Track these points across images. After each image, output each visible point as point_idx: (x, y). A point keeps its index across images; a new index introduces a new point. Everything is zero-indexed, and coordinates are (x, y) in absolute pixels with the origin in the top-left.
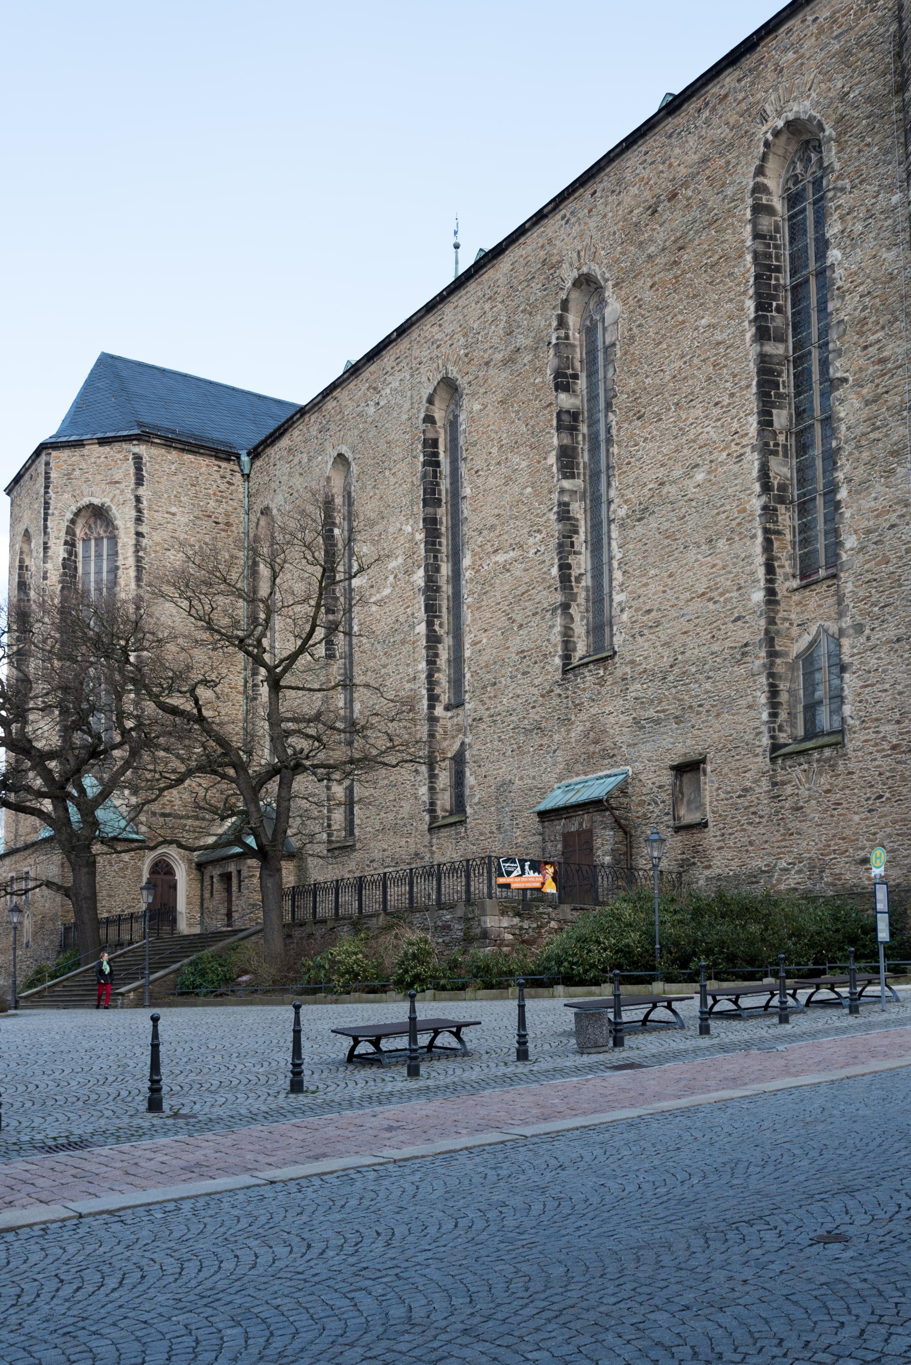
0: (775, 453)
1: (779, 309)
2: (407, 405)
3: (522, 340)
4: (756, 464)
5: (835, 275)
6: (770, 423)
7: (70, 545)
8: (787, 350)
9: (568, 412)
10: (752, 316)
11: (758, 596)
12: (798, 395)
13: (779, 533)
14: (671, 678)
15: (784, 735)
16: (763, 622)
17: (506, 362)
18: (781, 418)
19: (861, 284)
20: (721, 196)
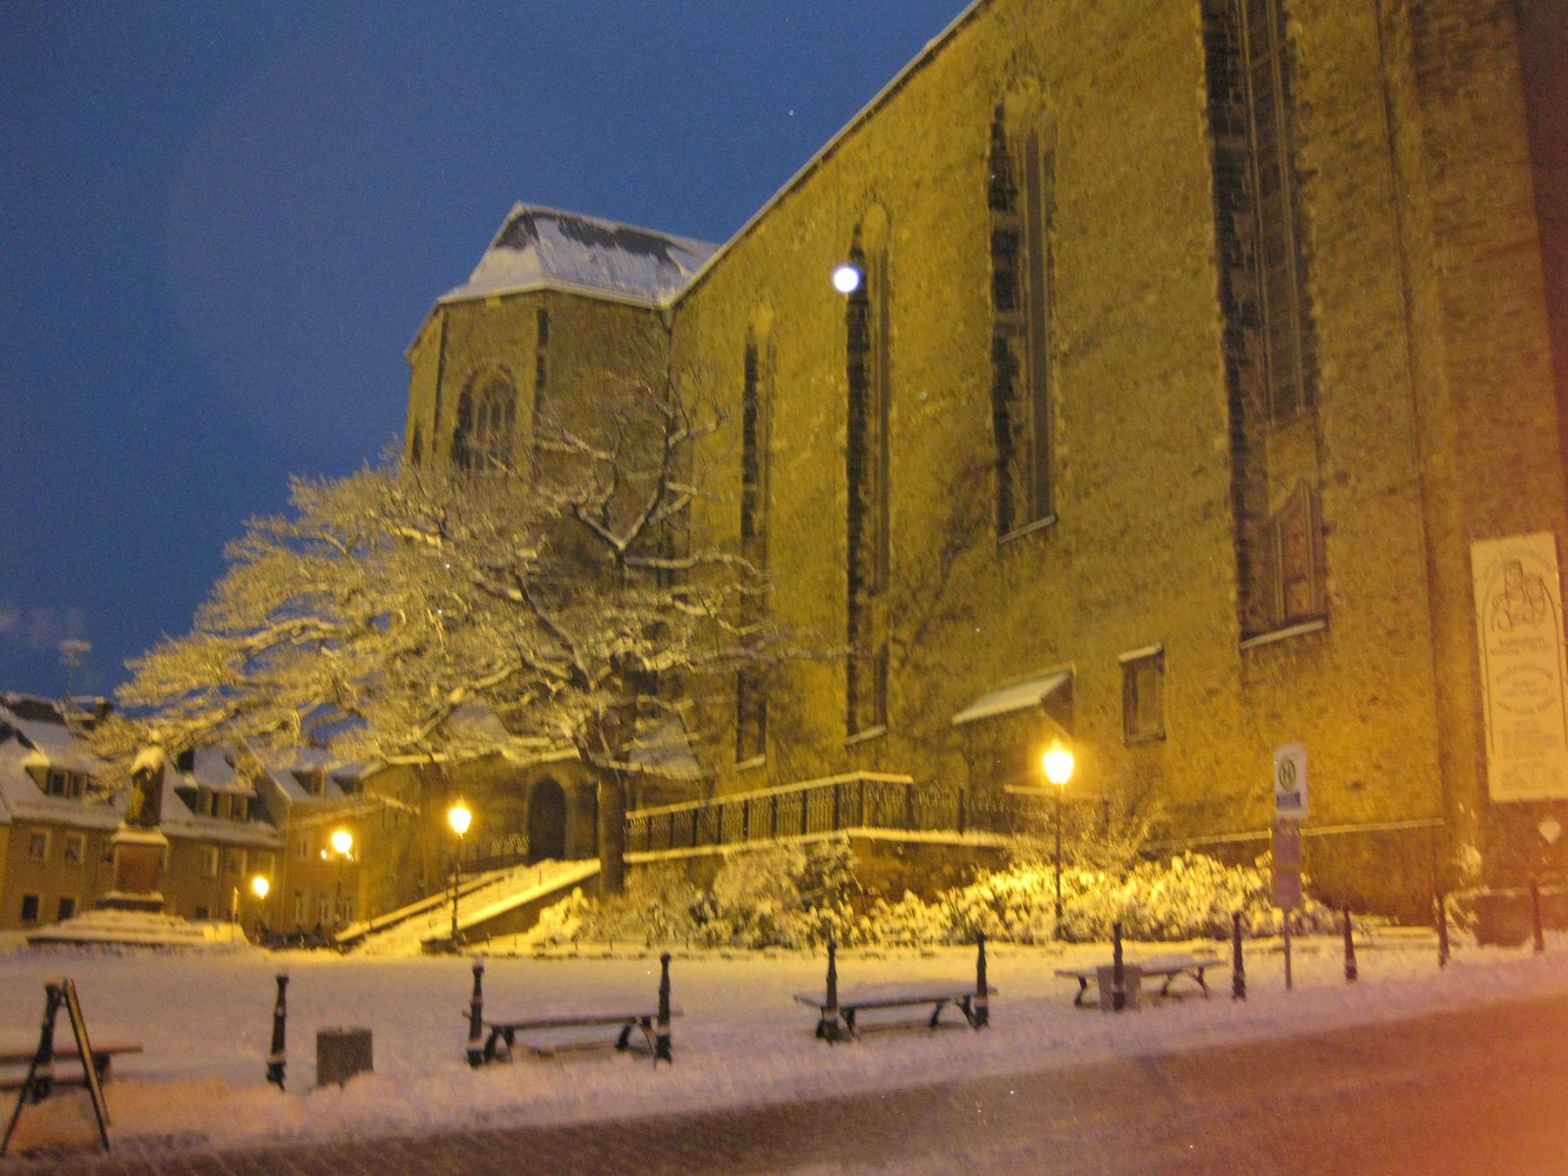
0: (1239, 266)
1: (1238, 98)
4: (1215, 280)
6: (1231, 230)
8: (1250, 145)
9: (1005, 233)
11: (1221, 442)
12: (1265, 194)
13: (1246, 363)
14: (1121, 548)
18: (1242, 224)
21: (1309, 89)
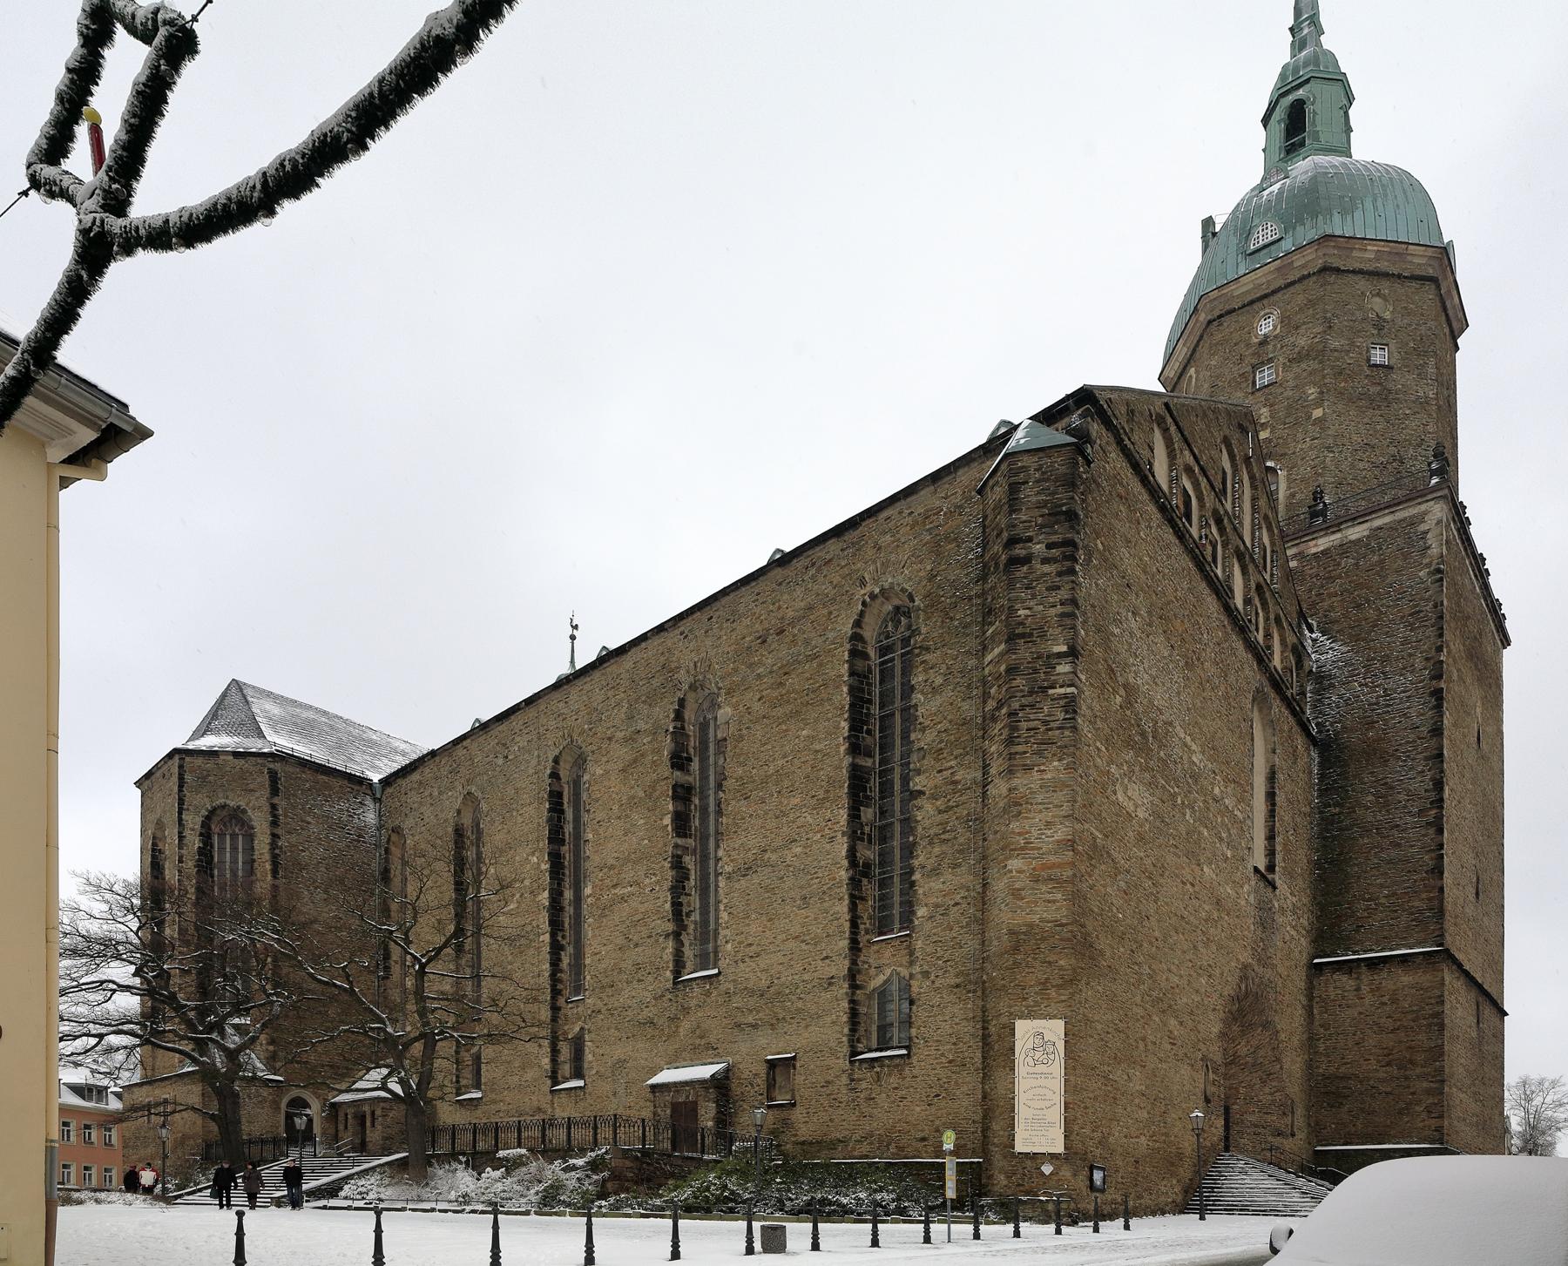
0: (863, 840)
1: (869, 732)
2: (534, 762)
3: (641, 725)
5: (919, 713)
6: (859, 817)
7: (206, 836)
8: (874, 761)
9: (682, 786)
10: (846, 734)
12: (881, 798)
13: (863, 899)
15: (861, 1045)
16: (847, 963)
17: (626, 740)
18: (868, 814)
19: (940, 723)
20: (823, 638)
21: (924, 739)
